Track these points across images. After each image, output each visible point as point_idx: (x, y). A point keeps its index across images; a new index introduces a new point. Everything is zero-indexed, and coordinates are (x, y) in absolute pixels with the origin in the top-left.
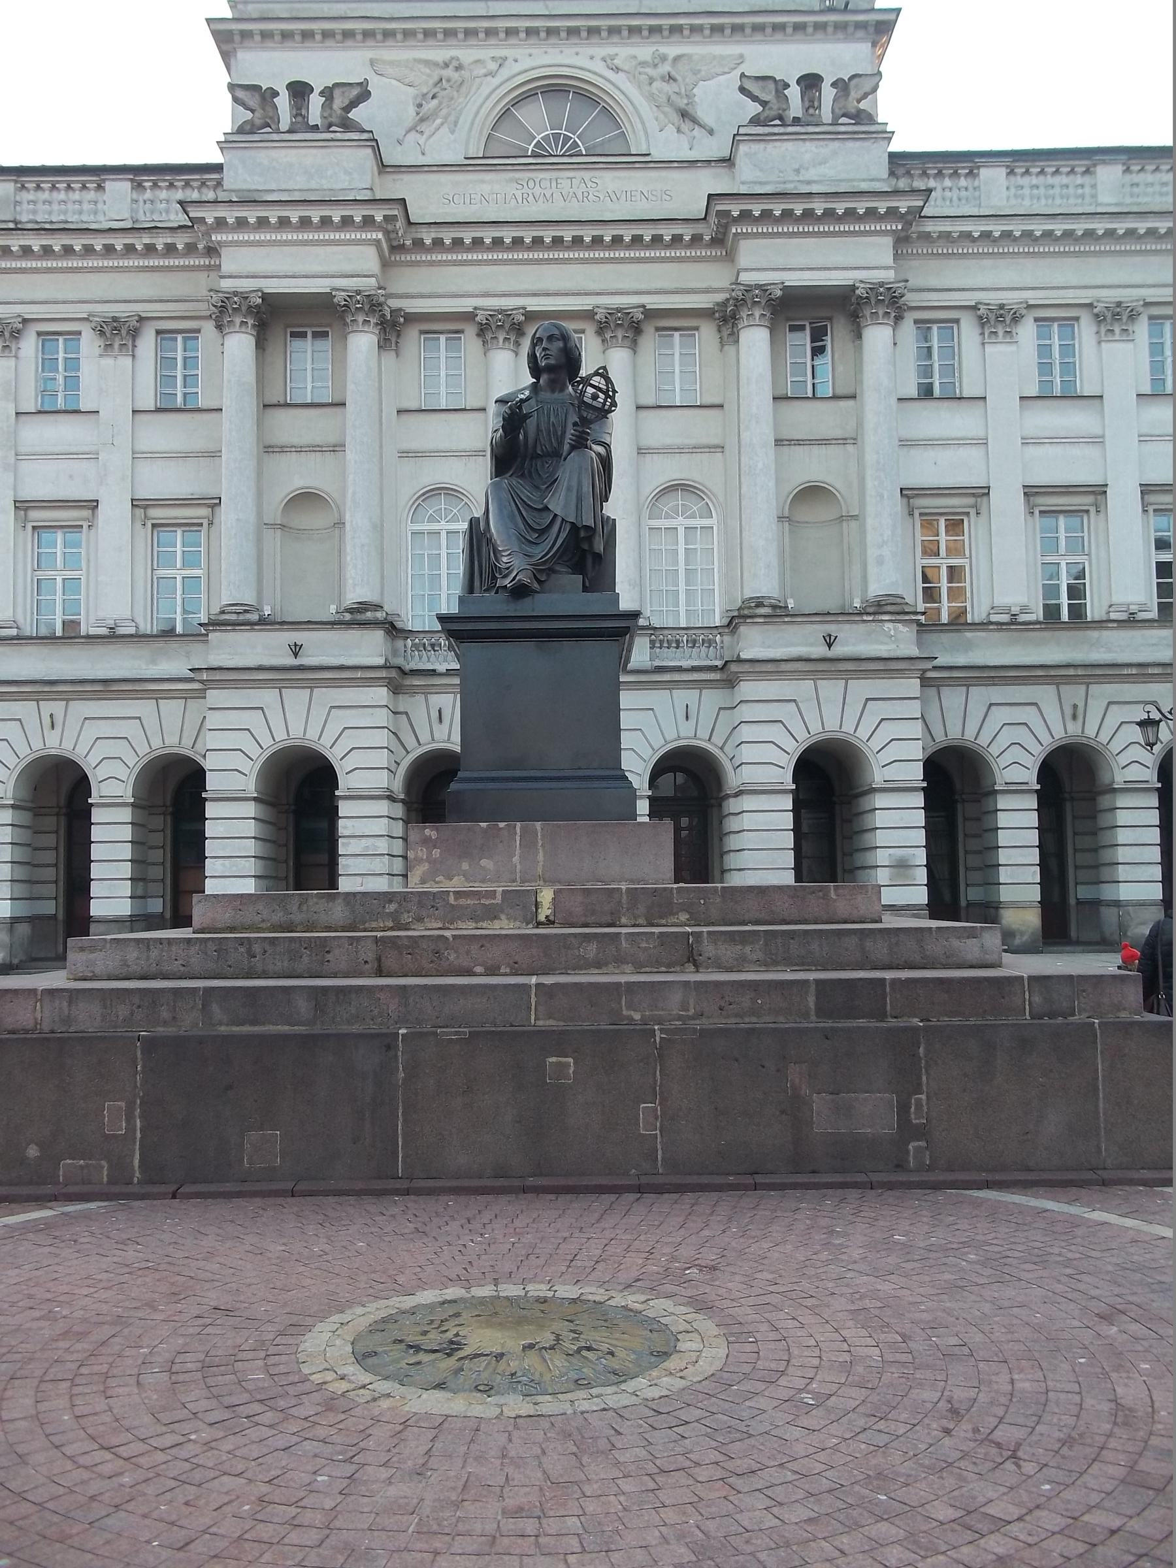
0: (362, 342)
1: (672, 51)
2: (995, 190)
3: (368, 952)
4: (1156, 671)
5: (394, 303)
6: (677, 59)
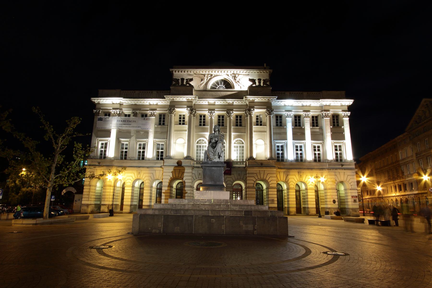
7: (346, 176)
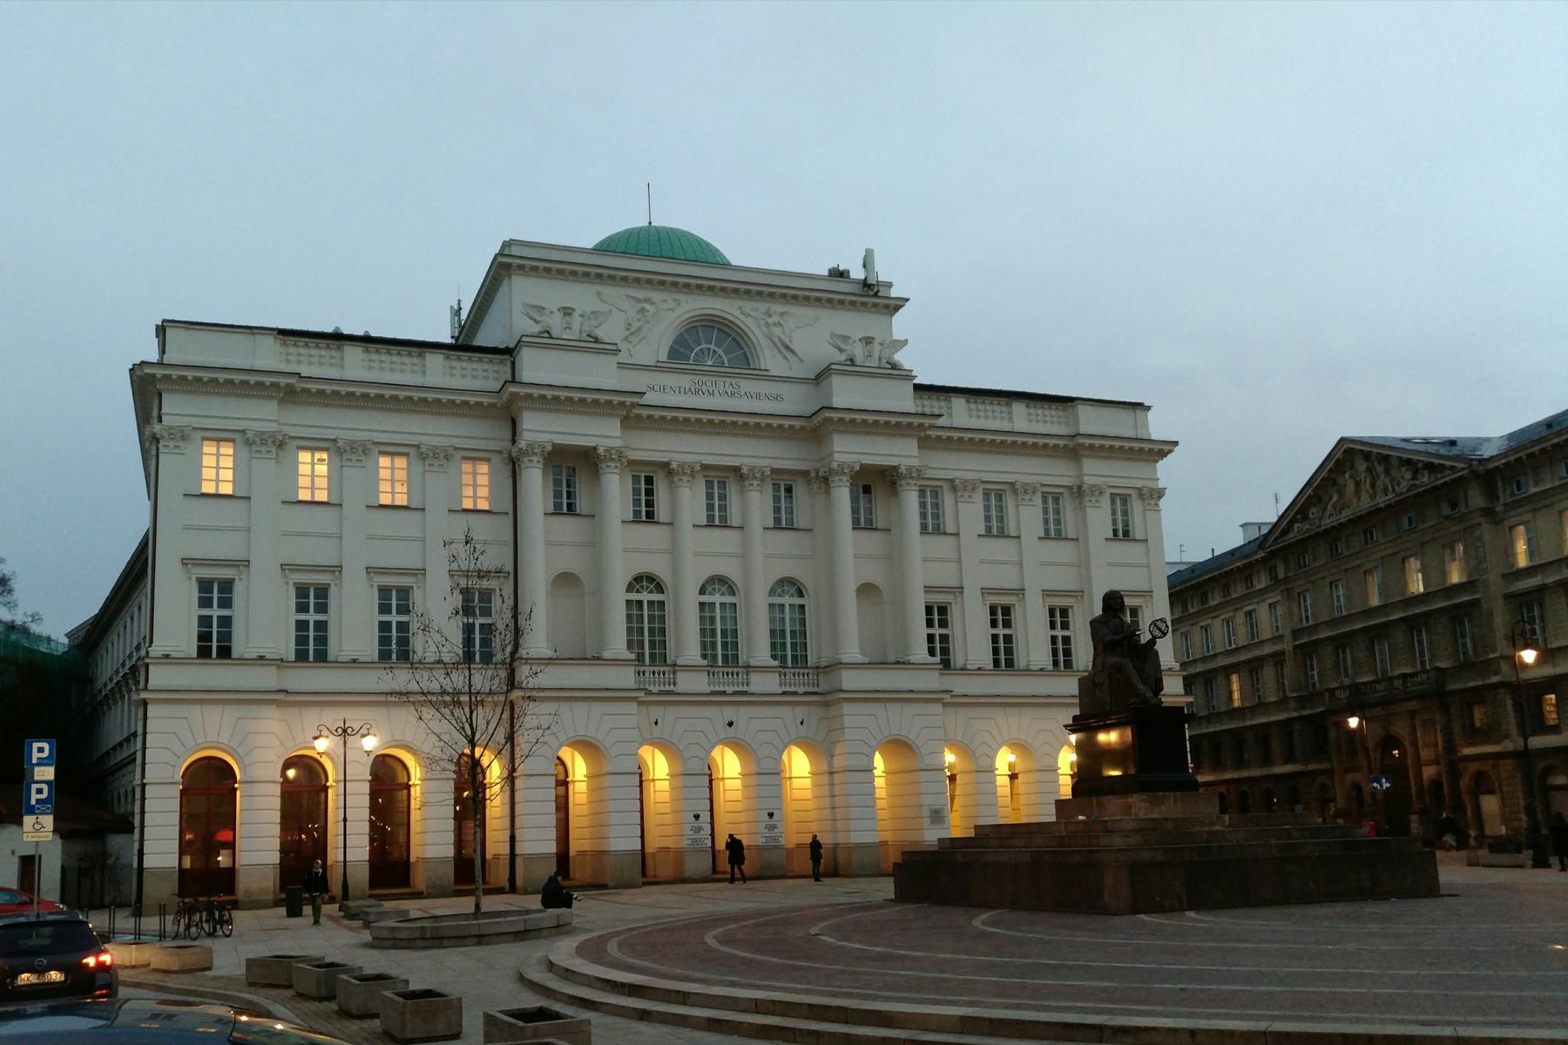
6: (782, 314)
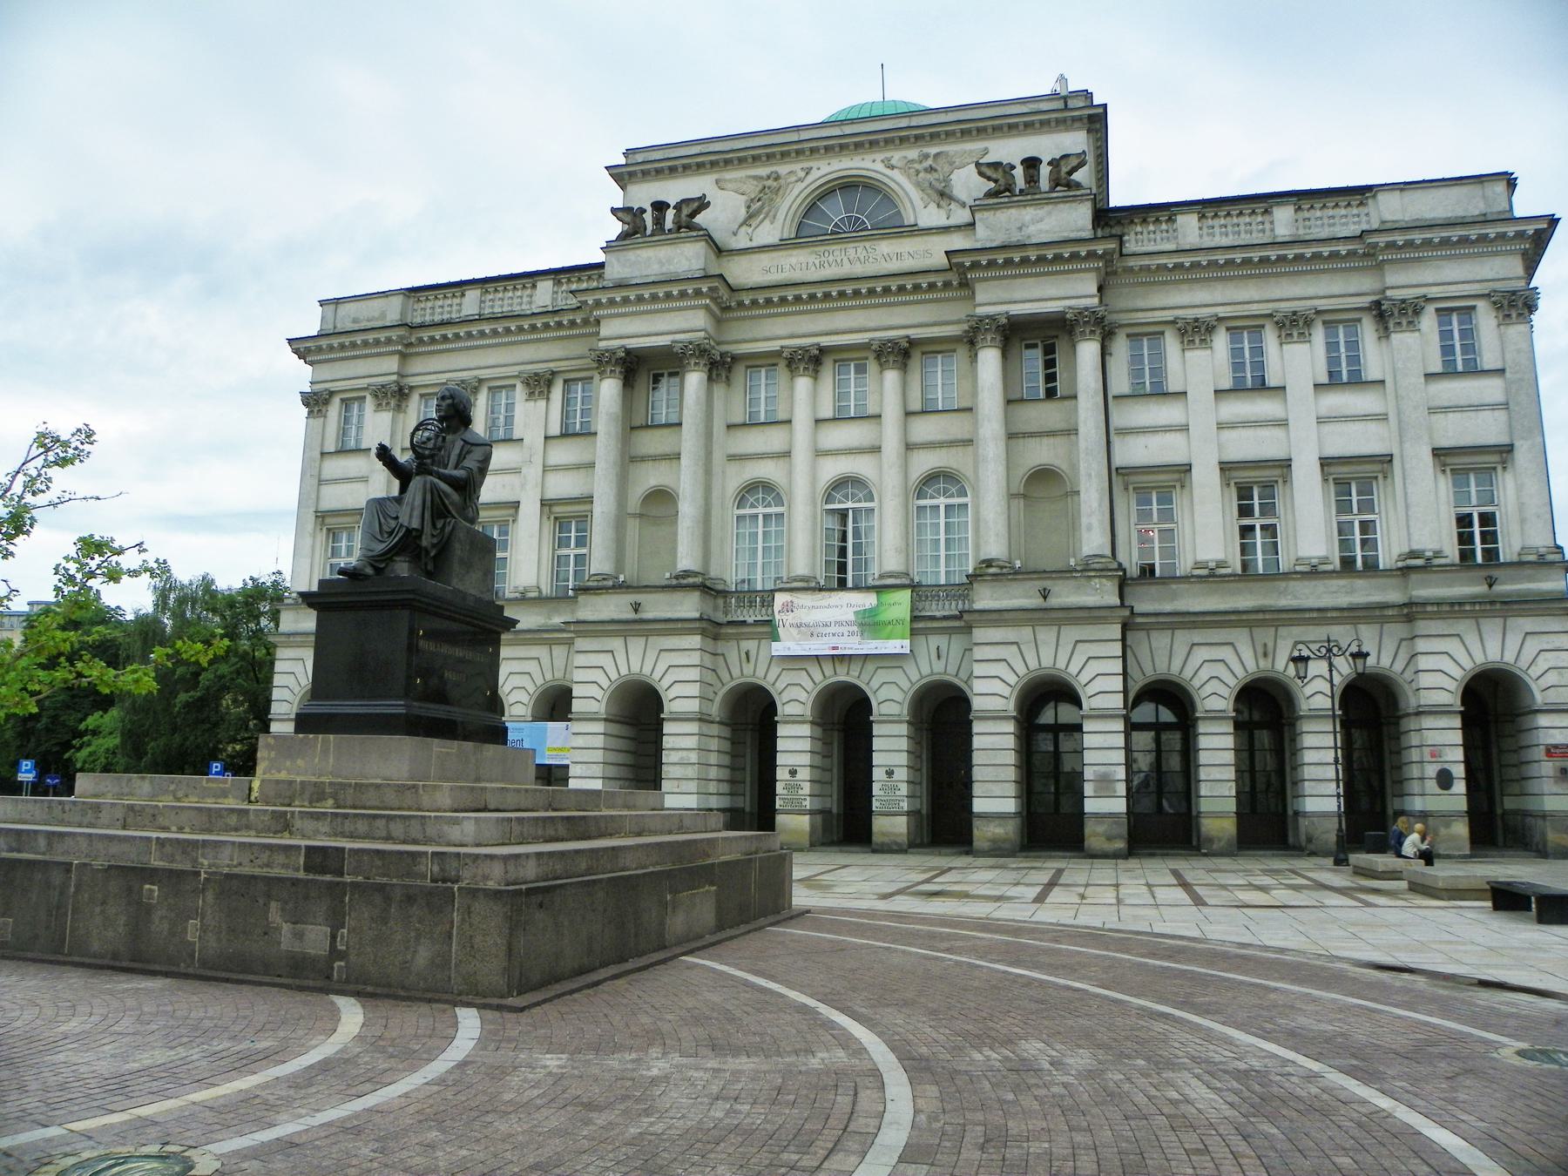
0: (694, 380)
1: (933, 150)
2: (1189, 229)
3: (119, 814)
4: (1335, 614)
5: (724, 348)
6: (937, 155)
7: (1513, 642)
